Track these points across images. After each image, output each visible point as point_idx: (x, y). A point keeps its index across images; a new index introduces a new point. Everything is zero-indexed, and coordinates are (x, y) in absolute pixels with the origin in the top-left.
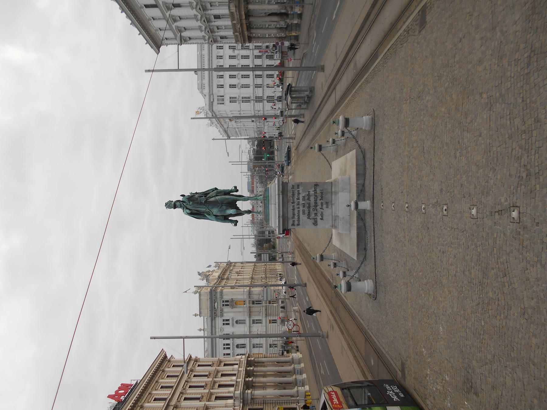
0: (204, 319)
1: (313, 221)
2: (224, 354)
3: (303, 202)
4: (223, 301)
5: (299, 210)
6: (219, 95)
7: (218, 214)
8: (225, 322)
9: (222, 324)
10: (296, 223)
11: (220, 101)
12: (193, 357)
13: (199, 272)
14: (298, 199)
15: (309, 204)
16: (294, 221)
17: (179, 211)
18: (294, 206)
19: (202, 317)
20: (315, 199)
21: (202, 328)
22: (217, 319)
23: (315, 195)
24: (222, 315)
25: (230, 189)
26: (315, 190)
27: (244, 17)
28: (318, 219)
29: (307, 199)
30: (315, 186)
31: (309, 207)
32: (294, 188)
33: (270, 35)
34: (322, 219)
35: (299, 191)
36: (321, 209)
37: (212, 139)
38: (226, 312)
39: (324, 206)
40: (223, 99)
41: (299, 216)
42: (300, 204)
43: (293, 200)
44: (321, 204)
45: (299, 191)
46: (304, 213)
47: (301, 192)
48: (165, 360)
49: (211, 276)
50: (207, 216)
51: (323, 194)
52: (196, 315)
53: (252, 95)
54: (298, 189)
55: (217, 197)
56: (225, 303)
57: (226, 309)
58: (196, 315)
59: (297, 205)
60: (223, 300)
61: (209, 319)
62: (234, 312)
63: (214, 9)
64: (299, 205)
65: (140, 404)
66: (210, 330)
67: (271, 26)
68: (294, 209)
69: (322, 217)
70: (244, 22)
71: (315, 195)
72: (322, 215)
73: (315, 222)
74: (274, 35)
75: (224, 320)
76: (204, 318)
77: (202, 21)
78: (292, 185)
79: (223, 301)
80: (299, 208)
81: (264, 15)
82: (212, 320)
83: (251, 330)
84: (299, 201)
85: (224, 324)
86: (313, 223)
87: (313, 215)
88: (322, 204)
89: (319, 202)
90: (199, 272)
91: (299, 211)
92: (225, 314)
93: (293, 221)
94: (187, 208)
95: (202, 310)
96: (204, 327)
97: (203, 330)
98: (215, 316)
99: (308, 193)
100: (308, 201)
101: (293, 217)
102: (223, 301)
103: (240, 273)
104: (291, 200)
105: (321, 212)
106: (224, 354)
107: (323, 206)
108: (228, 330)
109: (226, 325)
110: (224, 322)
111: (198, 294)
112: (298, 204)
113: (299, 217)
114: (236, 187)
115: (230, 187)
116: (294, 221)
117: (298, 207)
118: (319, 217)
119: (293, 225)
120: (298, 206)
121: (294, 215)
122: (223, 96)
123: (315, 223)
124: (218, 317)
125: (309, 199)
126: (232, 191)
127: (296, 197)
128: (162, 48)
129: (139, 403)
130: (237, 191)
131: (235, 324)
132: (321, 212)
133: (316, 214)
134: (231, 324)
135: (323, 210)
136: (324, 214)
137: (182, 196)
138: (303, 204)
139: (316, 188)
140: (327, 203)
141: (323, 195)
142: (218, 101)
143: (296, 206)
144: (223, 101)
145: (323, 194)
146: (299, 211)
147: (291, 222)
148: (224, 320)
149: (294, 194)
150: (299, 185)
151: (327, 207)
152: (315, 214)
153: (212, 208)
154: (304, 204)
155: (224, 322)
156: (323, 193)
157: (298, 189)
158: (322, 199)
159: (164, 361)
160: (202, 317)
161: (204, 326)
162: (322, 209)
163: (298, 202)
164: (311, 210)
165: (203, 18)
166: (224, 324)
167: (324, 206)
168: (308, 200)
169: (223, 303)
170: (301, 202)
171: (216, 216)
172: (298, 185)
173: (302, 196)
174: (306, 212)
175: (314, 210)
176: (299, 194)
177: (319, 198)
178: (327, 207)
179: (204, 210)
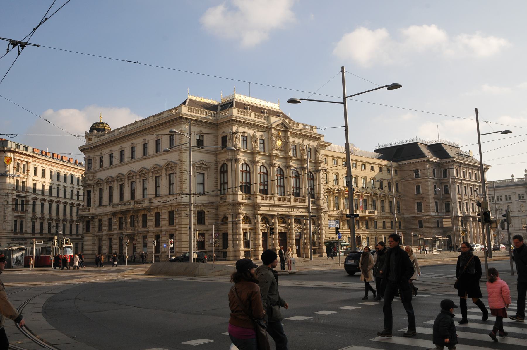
0: (523, 178)
9: (519, 194)
19: (524, 177)
21: (514, 178)
22: (524, 189)
61: (523, 183)
75: (523, 195)
76: (524, 178)
82: (522, 185)
96: (515, 179)
97: (513, 178)
108: (515, 198)
110: (521, 195)
155: (521, 195)
160: (524, 177)
161: (516, 179)
166: (519, 195)
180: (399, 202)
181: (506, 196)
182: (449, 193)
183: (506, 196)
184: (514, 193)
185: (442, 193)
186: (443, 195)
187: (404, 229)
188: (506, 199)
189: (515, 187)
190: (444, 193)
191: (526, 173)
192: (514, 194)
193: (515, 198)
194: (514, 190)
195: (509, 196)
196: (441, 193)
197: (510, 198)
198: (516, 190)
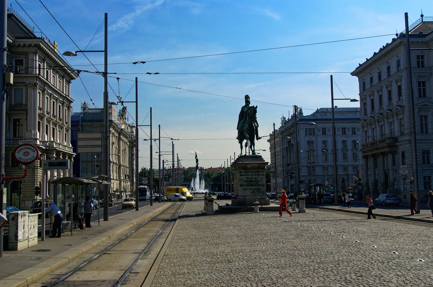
6: (315, 131)
7: (244, 128)
10: (242, 174)
11: (309, 131)
12: (72, 105)
14: (256, 175)
16: (243, 172)
17: (244, 104)
23: (258, 185)
25: (259, 135)
26: (261, 185)
27: (382, 151)
31: (251, 181)
33: (370, 175)
34: (244, 189)
37: (274, 123)
39: (251, 191)
40: (311, 134)
41: (246, 175)
42: (253, 176)
43: (255, 172)
46: (247, 178)
48: (70, 79)
50: (242, 121)
53: (316, 164)
55: (254, 127)
63: (388, 125)
65: (46, 58)
67: (377, 176)
68: (249, 172)
70: (379, 151)
74: (370, 179)
77: (379, 114)
81: (386, 168)
86: (241, 184)
87: (245, 183)
88: (253, 189)
89: (253, 187)
94: (248, 109)
100: (254, 181)
101: (245, 172)
114: (260, 138)
115: (260, 135)
116: (243, 172)
119: (240, 172)
121: (246, 172)
122: (314, 134)
123: (241, 185)
126: (257, 136)
127: (257, 173)
128: (356, 78)
129: (46, 57)
130: (258, 139)
133: (247, 185)
135: (250, 190)
137: (257, 106)
142: (309, 129)
143: (251, 174)
144: (309, 134)
147: (242, 171)
152: (247, 185)
153: (248, 124)
159: (70, 77)
164: (249, 183)
165: (381, 115)
170: (254, 177)
171: (243, 127)
174: (248, 180)
176: (259, 175)
179: (247, 119)
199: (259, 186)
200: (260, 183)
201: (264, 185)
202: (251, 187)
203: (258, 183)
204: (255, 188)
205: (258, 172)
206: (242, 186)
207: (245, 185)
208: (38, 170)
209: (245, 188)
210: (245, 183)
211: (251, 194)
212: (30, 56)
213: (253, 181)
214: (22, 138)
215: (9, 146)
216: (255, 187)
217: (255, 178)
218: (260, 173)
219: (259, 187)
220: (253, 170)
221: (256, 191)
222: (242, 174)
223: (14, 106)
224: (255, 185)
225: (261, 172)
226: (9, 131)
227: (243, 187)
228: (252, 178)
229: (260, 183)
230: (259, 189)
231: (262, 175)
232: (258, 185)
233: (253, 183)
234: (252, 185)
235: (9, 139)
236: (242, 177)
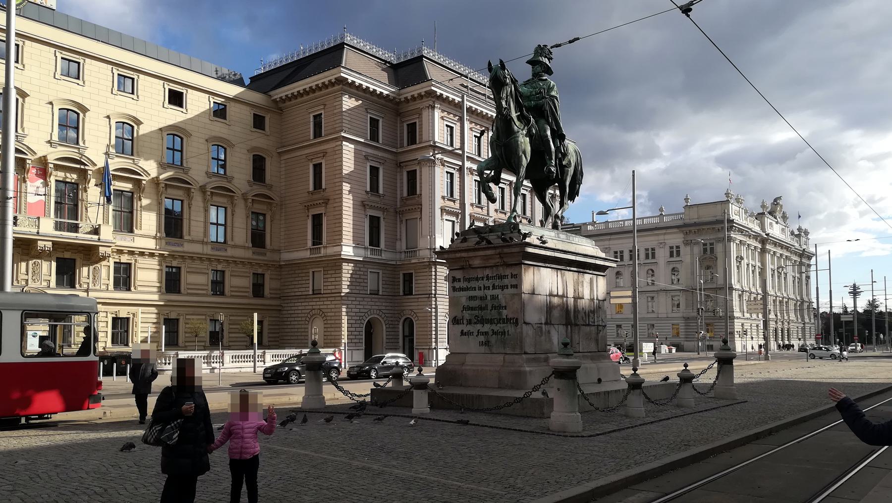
1: (459, 316)
2: (623, 251)
3: (489, 298)
4: (711, 244)
5: (477, 288)
8: (675, 250)
10: (457, 285)
13: (780, 198)
14: (494, 287)
15: (486, 308)
16: (459, 280)
18: (483, 280)
19: (683, 210)
20: (494, 319)
22: (681, 235)
23: (500, 319)
24: (687, 243)
26: (508, 320)
28: (462, 325)
29: (493, 304)
30: (514, 320)
31: (481, 308)
32: (512, 278)
34: (462, 333)
35: (507, 288)
36: (478, 332)
38: (692, 250)
39: (482, 338)
41: (467, 289)
44: (486, 332)
45: (507, 288)
46: (471, 298)
47: (505, 290)
49: (771, 221)
51: (502, 335)
52: (686, 200)
54: (509, 287)
56: (708, 247)
57: (697, 250)
58: (686, 200)
59: (484, 286)
60: (715, 243)
61: (680, 223)
62: (692, 264)
64: (484, 289)
66: (662, 225)
68: (477, 279)
69: (465, 332)
71: (500, 319)
72: (469, 334)
73: (458, 320)
75: (678, 247)
78: (517, 275)
79: (713, 243)
80: (480, 289)
83: (660, 294)
84: (491, 288)
85: (671, 248)
86: (455, 317)
87: (467, 315)
88: (486, 333)
89: (487, 328)
90: (780, 198)
91: (475, 290)
92: (688, 248)
93: (460, 279)
95: (695, 209)
97: (661, 214)
98: (685, 232)
99: (503, 307)
100: (489, 307)
101: (465, 280)
102: (711, 244)
103: (781, 274)
104: (493, 274)
105: (473, 332)
106: (623, 251)
107: (483, 335)
108: (662, 255)
109: (671, 251)
110: (675, 248)
111: (726, 199)
112: (485, 288)
113: (465, 291)
116: (459, 280)
117: (481, 287)
118: (466, 328)
120: (482, 289)
121: (469, 280)
124: (684, 238)
125: (494, 307)
127: (497, 282)
131: (671, 266)
132: (473, 332)
133: (470, 322)
134: (672, 259)
136: (471, 337)
138: (486, 297)
139: (512, 321)
140: (487, 343)
141: (499, 336)
143: (480, 283)
145: (502, 335)
146: (475, 290)
148: (678, 247)
149: (502, 279)
150: (517, 288)
151: (481, 344)
152: (470, 320)
154: (486, 299)
155: (675, 248)
156: (503, 336)
157: (509, 287)
158: (494, 333)
160: (683, 210)
162: (478, 334)
163: (489, 287)
166: (671, 248)
167: (482, 338)
168: (492, 307)
169: (708, 245)
172: (517, 285)
173: (498, 295)
175: (476, 318)
176: (503, 288)
177: (496, 328)
178: (481, 344)
180: (264, 215)
181: (647, 250)
182: (418, 192)
183: (647, 250)
184: (662, 244)
185: (402, 194)
186: (402, 198)
187: (271, 298)
188: (647, 257)
189: (664, 231)
190: (405, 194)
191: (687, 202)
192: (661, 246)
193: (662, 255)
194: (661, 237)
195: (653, 249)
196: (398, 193)
197: (653, 257)
198: (667, 237)
199: (504, 323)
200: (505, 312)
201: (517, 319)
202: (479, 326)
203: (500, 314)
204: (493, 330)
205: (501, 277)
206: (458, 323)
207: (465, 322)
208: (438, 299)
209: (466, 328)
210: (467, 315)
211: (483, 349)
212: (425, 114)
213: (486, 308)
214: (416, 249)
215: (398, 263)
216: (494, 327)
217: (494, 298)
218: (506, 281)
219: (502, 325)
220: (488, 272)
221: (493, 339)
222: (457, 285)
223: (406, 199)
224: (491, 322)
225: (509, 277)
226: (401, 239)
227: (460, 327)
228: (483, 298)
229: (505, 312)
230: (503, 333)
231: (511, 285)
232: (501, 320)
233: (488, 314)
234: (483, 321)
235: (401, 253)
236: (457, 294)
